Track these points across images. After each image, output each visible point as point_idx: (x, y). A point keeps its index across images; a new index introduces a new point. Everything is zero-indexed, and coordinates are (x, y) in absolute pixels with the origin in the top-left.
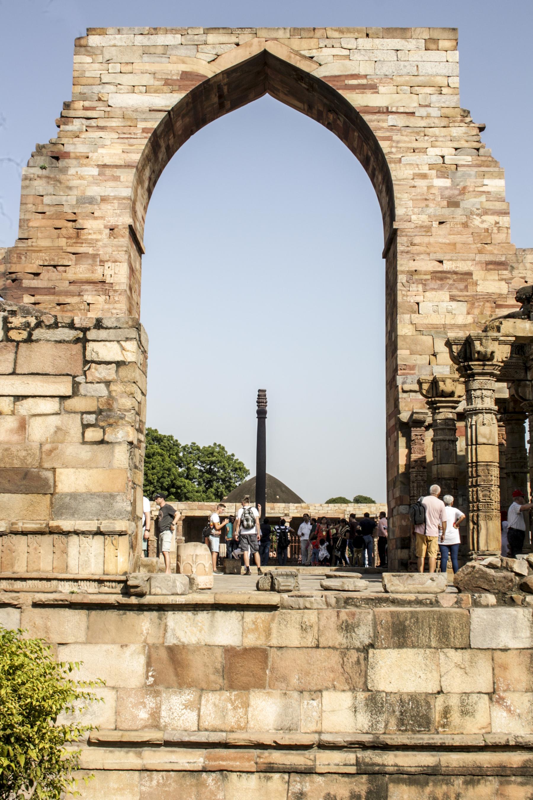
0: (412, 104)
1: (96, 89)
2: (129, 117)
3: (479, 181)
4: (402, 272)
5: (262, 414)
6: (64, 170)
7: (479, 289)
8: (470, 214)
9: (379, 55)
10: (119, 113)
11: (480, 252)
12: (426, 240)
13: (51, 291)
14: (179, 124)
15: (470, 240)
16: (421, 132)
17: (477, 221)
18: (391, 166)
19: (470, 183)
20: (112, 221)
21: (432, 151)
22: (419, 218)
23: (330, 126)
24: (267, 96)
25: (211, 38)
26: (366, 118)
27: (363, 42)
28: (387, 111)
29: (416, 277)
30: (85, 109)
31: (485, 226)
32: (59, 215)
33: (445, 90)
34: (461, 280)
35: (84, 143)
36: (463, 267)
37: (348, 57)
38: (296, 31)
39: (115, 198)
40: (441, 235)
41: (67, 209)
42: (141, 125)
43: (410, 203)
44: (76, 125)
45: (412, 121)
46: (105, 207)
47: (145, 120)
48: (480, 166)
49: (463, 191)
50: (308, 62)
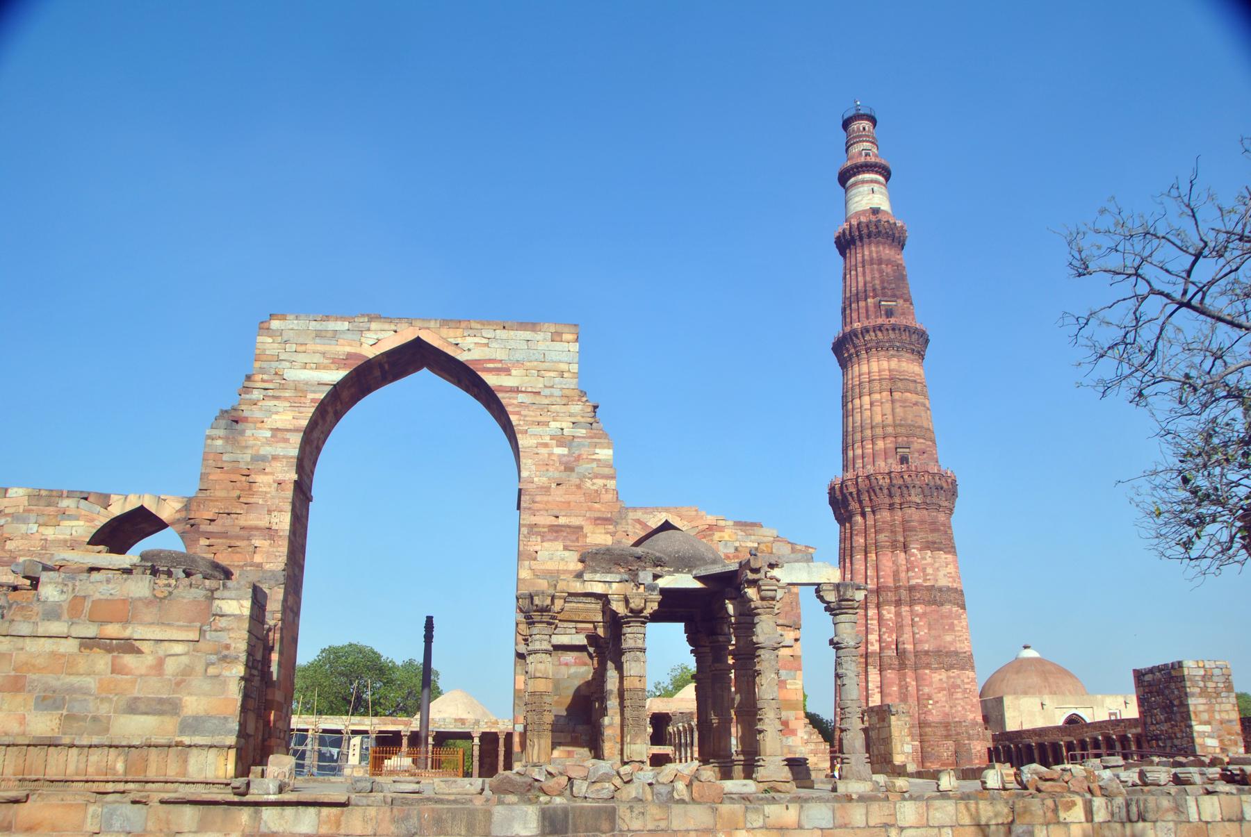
0: (539, 385)
1: (274, 364)
2: (300, 389)
3: (591, 450)
4: (525, 525)
5: (429, 638)
6: (242, 432)
7: (588, 540)
8: (582, 478)
9: (512, 344)
10: (292, 384)
11: (590, 509)
12: (545, 498)
13: (224, 535)
14: (345, 395)
15: (582, 499)
16: (546, 408)
17: (588, 484)
18: (519, 436)
19: (584, 452)
20: (280, 477)
21: (553, 425)
22: (540, 480)
23: (476, 397)
24: (425, 371)
25: (374, 326)
26: (500, 395)
27: (501, 334)
28: (517, 390)
29: (535, 530)
30: (263, 381)
31: (595, 487)
32: (235, 471)
33: (566, 375)
34: (574, 533)
35: (260, 410)
36: (575, 521)
37: (487, 345)
38: (445, 323)
39: (285, 457)
40: (558, 495)
41: (242, 465)
42: (311, 396)
43: (533, 467)
44: (256, 395)
45: (538, 399)
46: (275, 464)
47: (314, 392)
48: (591, 437)
49: (578, 458)
50: (454, 348)
